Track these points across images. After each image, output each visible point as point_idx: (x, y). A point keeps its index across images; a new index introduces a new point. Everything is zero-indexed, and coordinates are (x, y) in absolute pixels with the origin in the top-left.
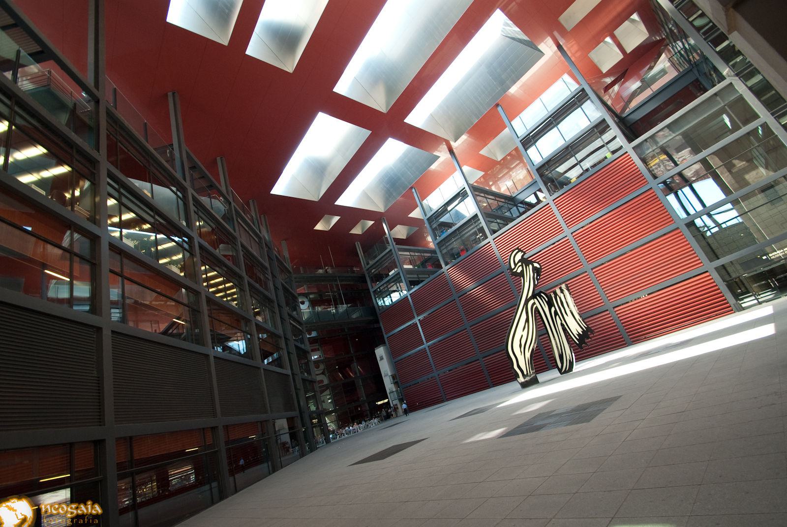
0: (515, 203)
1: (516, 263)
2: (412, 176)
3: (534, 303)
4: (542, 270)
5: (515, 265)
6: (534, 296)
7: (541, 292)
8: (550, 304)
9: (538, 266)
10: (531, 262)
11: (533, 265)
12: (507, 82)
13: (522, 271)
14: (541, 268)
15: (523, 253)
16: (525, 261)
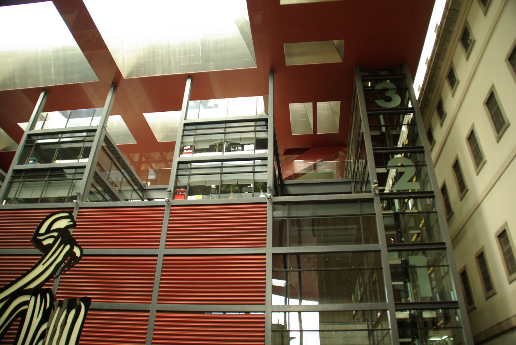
0: (143, 196)
1: (54, 227)
2: (53, 77)
3: (27, 303)
4: (80, 262)
5: (48, 231)
6: (34, 292)
7: (49, 291)
8: (46, 318)
9: (78, 254)
10: (73, 243)
11: (72, 248)
12: (212, 63)
13: (50, 246)
14: (80, 258)
15: (71, 223)
16: (64, 236)
